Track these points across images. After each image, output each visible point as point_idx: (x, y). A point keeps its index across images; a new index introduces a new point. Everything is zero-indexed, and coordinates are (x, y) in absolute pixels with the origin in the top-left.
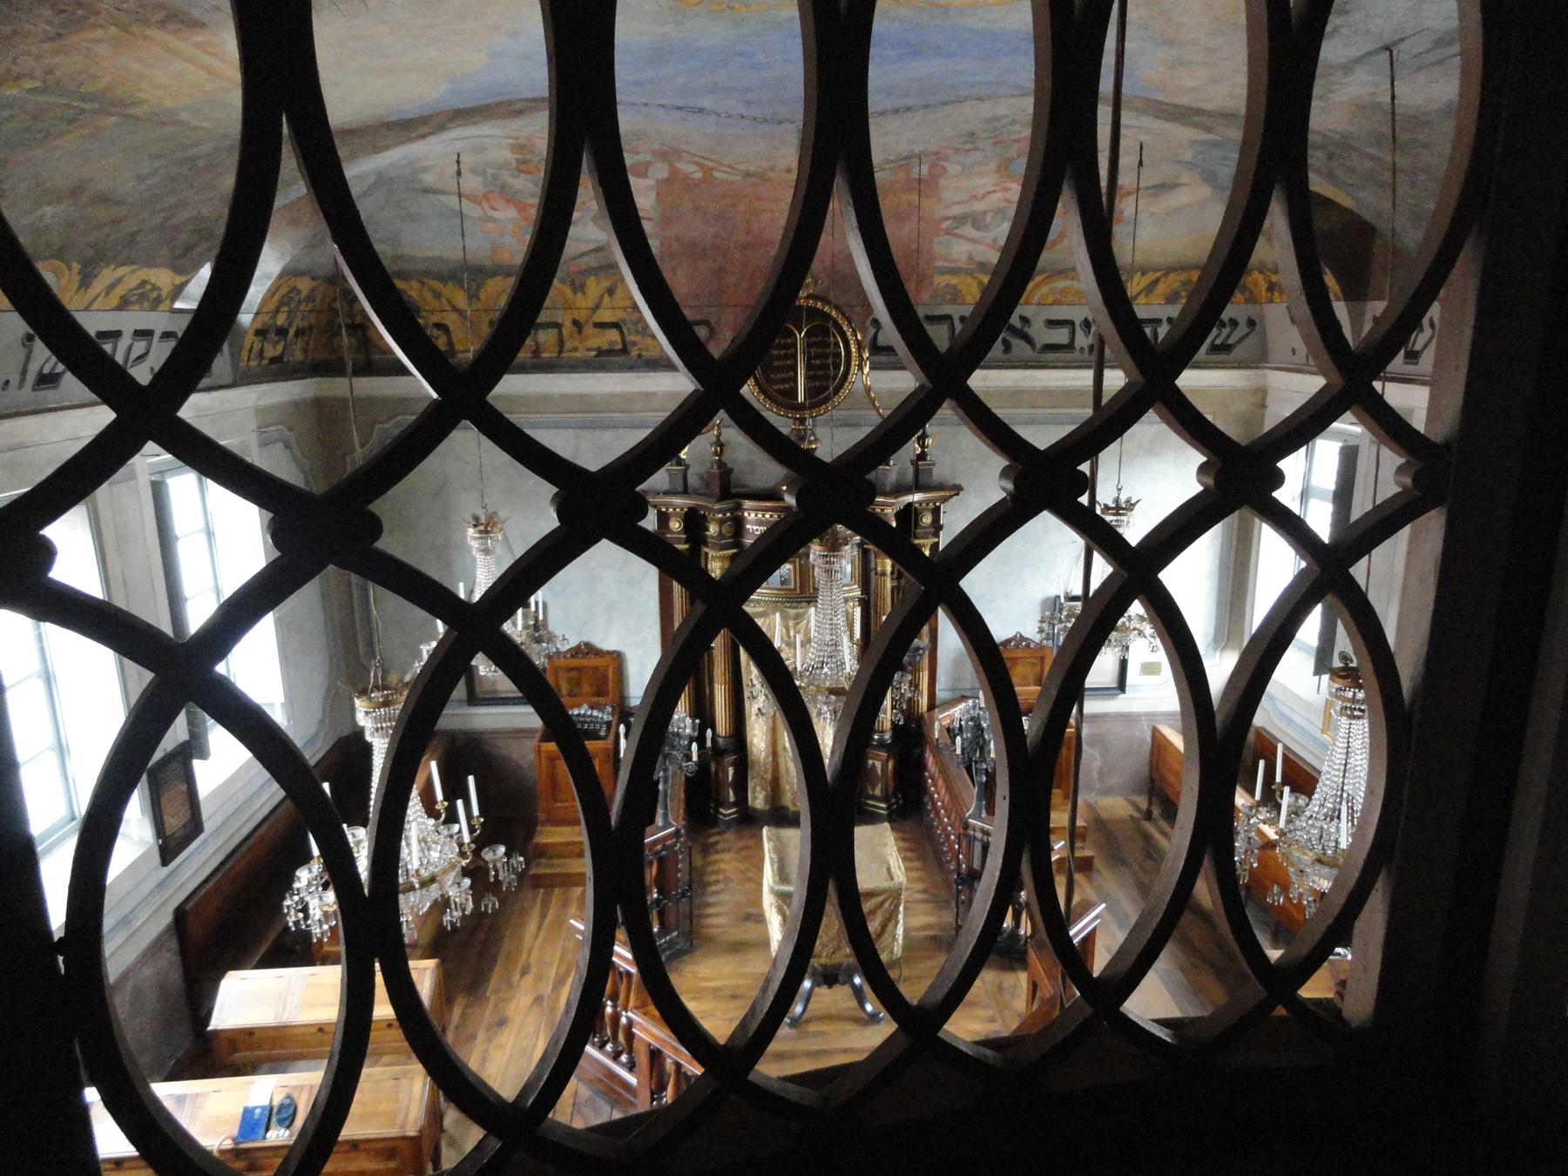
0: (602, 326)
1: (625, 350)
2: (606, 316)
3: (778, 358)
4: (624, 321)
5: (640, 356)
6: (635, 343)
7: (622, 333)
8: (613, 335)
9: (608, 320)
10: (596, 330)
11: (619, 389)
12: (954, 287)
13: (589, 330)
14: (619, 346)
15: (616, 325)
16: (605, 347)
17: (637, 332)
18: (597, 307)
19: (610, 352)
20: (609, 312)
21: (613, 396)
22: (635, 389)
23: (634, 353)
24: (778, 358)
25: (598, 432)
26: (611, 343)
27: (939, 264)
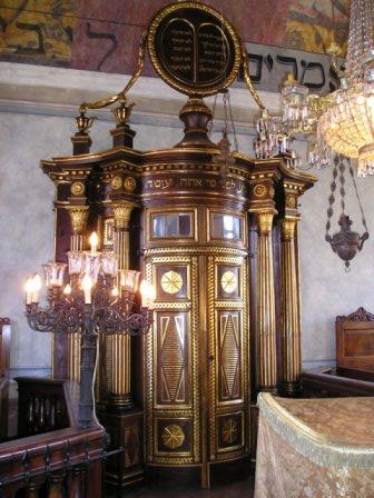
0: (22, 26)
1: (41, 50)
2: (29, 18)
3: (177, 45)
4: (43, 25)
5: (53, 57)
6: (51, 46)
7: (40, 36)
8: (33, 36)
9: (30, 22)
10: (21, 31)
11: (34, 82)
12: (299, 34)
13: (12, 29)
14: (37, 47)
15: (36, 28)
16: (25, 46)
17: (53, 36)
18: (21, 9)
19: (29, 50)
20: (31, 15)
21: (26, 87)
22: (48, 84)
23: (49, 55)
24: (177, 45)
25: (9, 115)
26: (31, 43)
27: (292, 8)
